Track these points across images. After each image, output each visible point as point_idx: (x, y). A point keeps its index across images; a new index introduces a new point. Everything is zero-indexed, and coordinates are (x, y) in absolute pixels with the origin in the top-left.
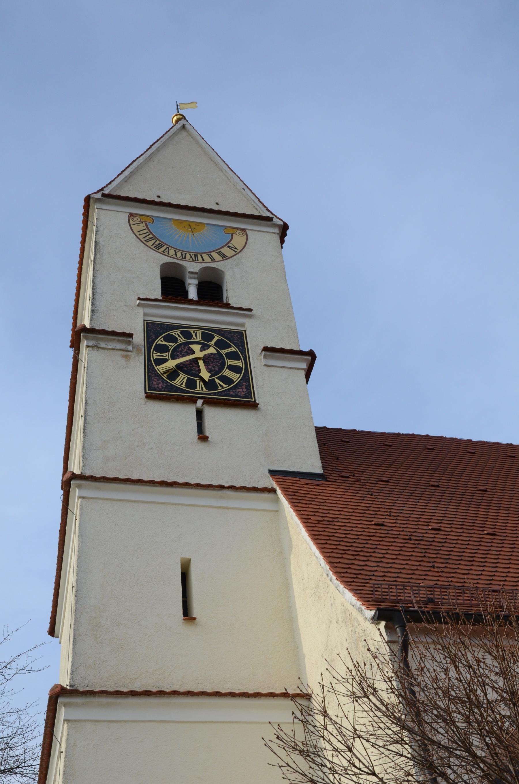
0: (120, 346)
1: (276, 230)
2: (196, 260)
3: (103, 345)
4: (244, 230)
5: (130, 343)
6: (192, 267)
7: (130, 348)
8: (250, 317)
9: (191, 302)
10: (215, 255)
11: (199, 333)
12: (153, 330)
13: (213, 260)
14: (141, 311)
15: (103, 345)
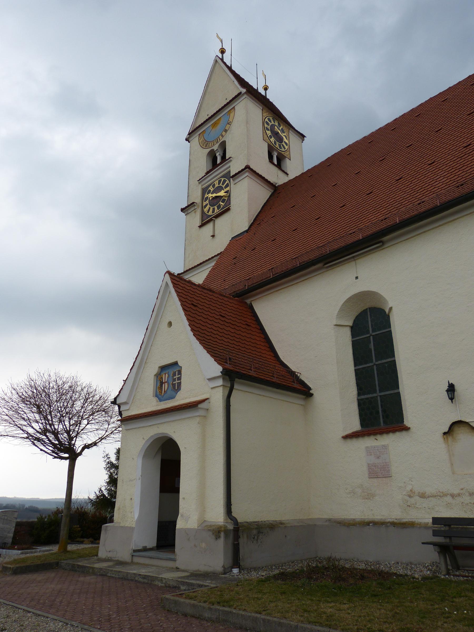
0: (193, 209)
1: (245, 96)
2: (217, 142)
3: (189, 212)
4: (234, 107)
5: (195, 205)
6: (215, 147)
7: (196, 207)
8: (231, 161)
9: (221, 163)
10: (224, 133)
11: (217, 182)
12: (205, 191)
13: (223, 136)
14: (200, 185)
15: (189, 212)
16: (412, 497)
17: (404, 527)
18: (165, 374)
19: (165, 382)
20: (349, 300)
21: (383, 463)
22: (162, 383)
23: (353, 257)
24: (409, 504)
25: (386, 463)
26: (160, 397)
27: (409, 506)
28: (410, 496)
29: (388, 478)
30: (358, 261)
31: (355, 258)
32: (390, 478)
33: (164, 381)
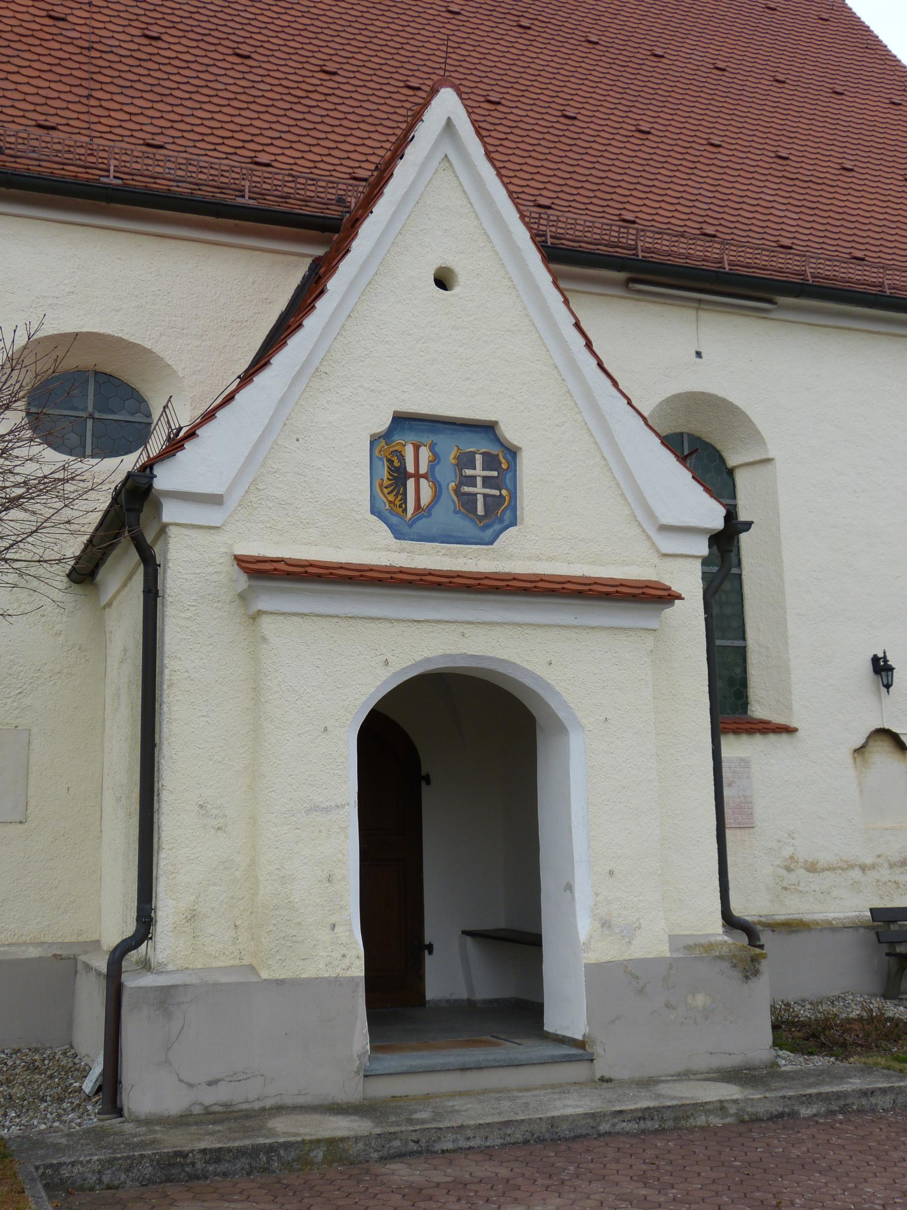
16: (793, 870)
17: (793, 932)
18: (417, 448)
19: (417, 476)
20: (668, 401)
21: (739, 797)
22: (399, 477)
23: (700, 301)
24: (785, 884)
25: (745, 796)
26: (395, 520)
27: (785, 889)
28: (789, 869)
29: (747, 831)
30: (704, 315)
31: (702, 306)
32: (751, 831)
33: (410, 469)
